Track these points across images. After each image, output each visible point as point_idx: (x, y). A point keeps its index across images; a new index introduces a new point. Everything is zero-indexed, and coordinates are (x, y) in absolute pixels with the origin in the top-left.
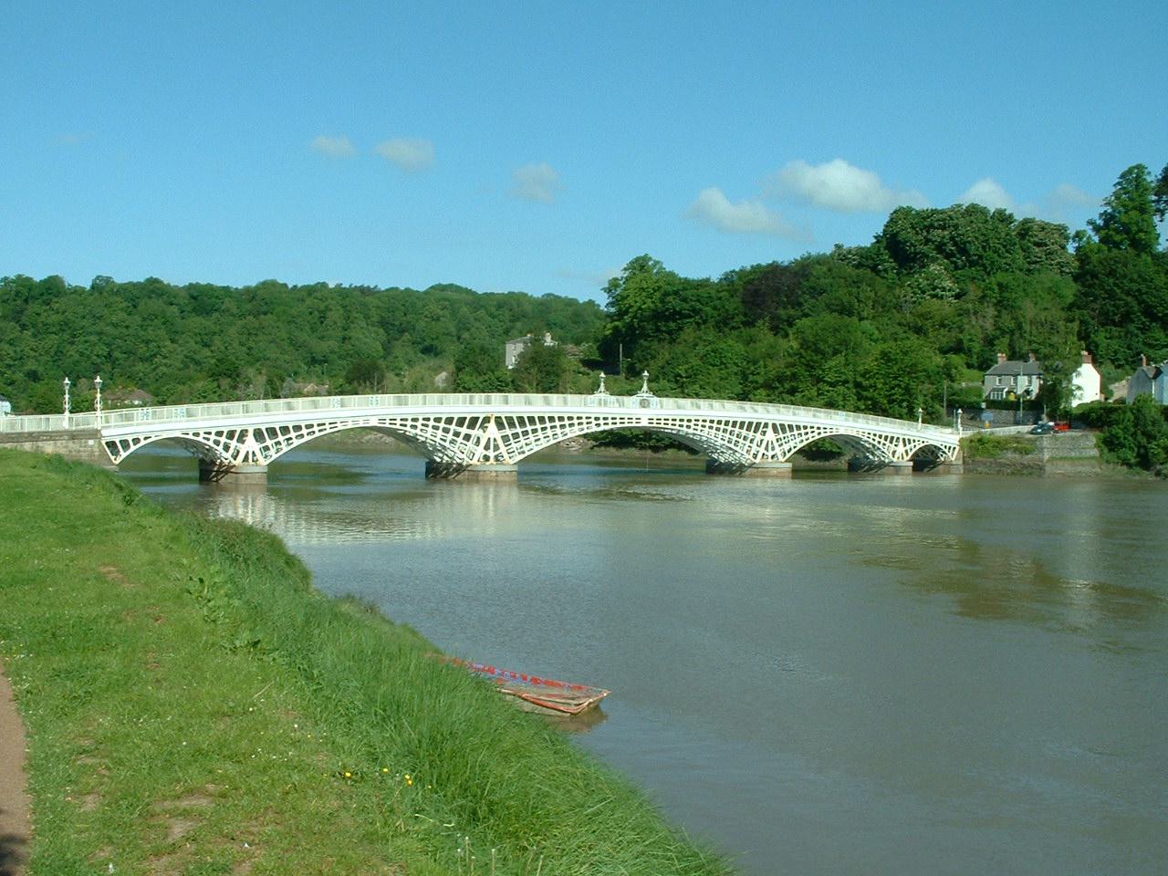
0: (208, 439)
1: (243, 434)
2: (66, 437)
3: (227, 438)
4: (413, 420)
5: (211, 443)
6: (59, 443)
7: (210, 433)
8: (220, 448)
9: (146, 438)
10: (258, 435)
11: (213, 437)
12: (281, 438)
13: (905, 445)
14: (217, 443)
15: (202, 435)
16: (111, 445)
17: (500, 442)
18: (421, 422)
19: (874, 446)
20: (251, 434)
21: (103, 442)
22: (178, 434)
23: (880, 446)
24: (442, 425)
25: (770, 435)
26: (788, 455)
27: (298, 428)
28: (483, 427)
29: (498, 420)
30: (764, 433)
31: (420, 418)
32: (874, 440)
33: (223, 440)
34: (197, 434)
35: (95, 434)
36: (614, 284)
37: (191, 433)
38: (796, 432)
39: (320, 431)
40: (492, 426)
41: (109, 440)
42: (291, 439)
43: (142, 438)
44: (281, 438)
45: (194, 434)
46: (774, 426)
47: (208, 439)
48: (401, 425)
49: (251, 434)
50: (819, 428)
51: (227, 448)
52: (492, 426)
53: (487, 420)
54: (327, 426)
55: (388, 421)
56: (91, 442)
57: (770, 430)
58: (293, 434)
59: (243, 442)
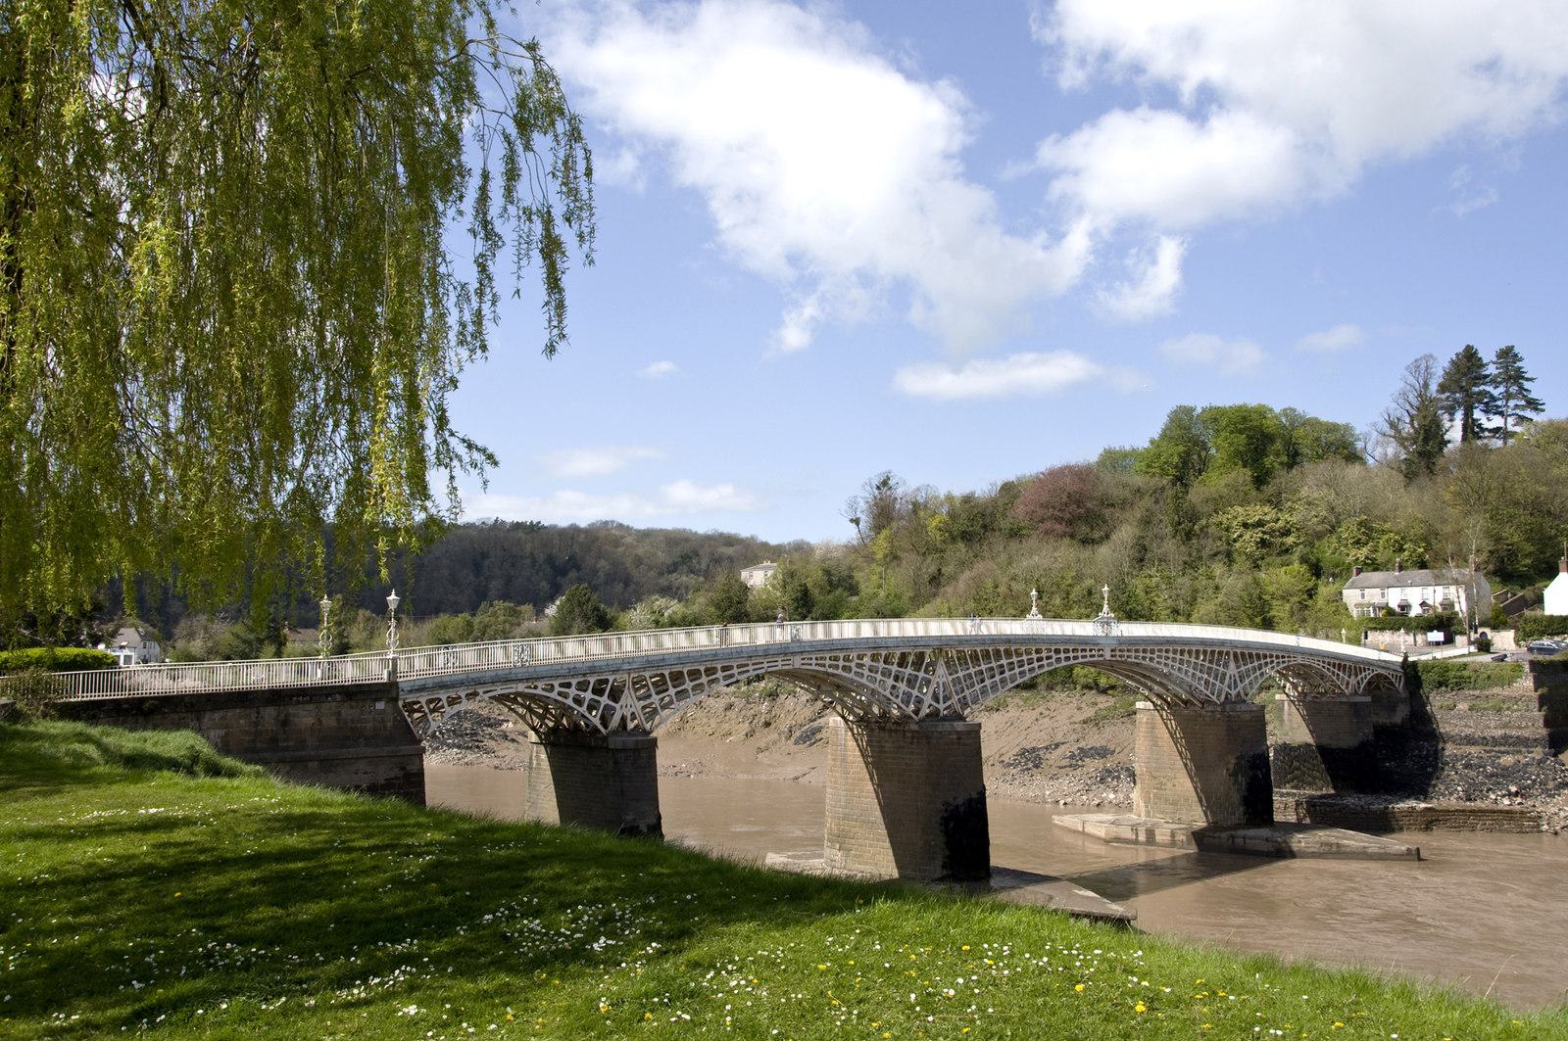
0: (566, 696)
3: (594, 692)
7: (568, 685)
8: (583, 709)
11: (573, 692)
12: (672, 691)
14: (578, 701)
15: (557, 689)
22: (521, 687)
25: (1232, 670)
30: (1226, 665)
33: (588, 695)
35: (388, 690)
38: (1256, 664)
41: (411, 698)
42: (685, 691)
46: (1235, 654)
47: (566, 696)
50: (1277, 657)
55: (814, 662)
56: (380, 705)
57: (1232, 665)
58: (688, 685)
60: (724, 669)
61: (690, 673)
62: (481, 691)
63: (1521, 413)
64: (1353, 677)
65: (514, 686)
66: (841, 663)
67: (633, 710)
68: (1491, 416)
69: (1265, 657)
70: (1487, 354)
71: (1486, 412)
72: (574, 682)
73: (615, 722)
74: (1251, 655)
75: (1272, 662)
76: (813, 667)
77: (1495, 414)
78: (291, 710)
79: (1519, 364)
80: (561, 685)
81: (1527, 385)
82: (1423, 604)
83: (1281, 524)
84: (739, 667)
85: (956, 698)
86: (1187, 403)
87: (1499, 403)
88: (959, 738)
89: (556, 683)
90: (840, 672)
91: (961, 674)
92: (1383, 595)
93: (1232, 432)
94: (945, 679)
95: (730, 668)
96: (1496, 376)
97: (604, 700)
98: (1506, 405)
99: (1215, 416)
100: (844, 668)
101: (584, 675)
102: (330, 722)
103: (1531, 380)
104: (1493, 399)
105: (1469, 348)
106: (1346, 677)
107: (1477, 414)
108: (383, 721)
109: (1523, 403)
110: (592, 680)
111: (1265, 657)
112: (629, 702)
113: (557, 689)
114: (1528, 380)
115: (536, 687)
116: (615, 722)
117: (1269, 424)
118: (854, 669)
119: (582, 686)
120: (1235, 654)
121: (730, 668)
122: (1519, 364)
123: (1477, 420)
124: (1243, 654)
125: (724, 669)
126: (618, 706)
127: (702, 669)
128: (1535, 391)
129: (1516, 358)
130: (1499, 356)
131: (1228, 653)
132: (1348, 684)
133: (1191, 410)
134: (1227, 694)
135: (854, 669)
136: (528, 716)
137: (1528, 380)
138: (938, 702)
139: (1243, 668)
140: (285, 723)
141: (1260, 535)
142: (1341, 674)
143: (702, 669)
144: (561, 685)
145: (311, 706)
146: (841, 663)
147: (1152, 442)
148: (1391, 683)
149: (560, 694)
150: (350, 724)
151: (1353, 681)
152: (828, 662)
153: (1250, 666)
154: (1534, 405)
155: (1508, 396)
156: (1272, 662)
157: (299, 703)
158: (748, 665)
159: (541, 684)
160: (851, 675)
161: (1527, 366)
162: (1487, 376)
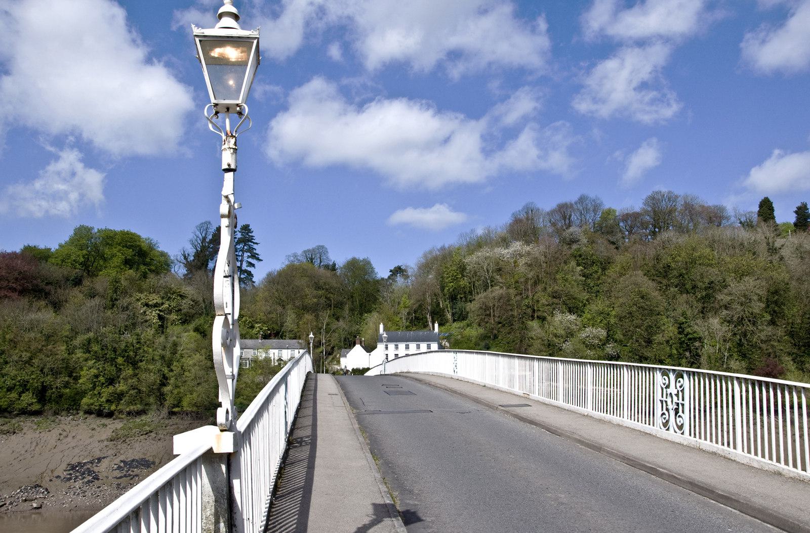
63: (250, 260)
79: (250, 234)
81: (255, 246)
83: (166, 306)
93: (123, 247)
98: (242, 256)
99: (110, 238)
103: (257, 243)
109: (250, 255)
114: (254, 243)
128: (258, 249)
129: (250, 231)
137: (254, 243)
141: (157, 312)
147: (61, 246)
161: (257, 235)
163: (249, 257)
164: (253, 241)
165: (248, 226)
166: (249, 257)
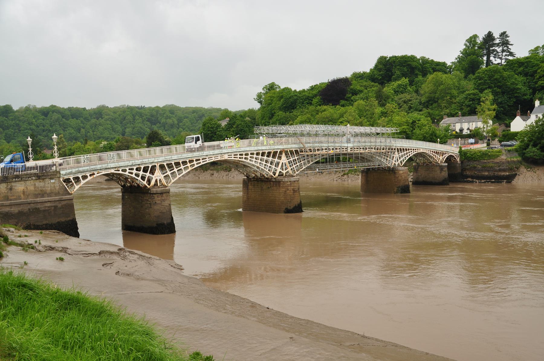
0: (132, 173)
1: (153, 168)
2: (34, 178)
3: (144, 171)
4: (251, 154)
5: (133, 176)
6: (28, 183)
7: (132, 169)
8: (139, 178)
9: (90, 175)
10: (162, 167)
11: (134, 172)
12: (176, 170)
13: (442, 156)
14: (137, 175)
15: (128, 171)
16: (67, 181)
17: (288, 165)
18: (250, 155)
19: (430, 156)
20: (158, 167)
21: (61, 179)
22: (113, 171)
23: (434, 157)
24: (255, 156)
26: (403, 163)
27: (184, 163)
28: (280, 158)
29: (286, 154)
31: (249, 153)
32: (432, 154)
33: (141, 173)
34: (125, 171)
36: (259, 96)
37: (121, 169)
38: (405, 152)
39: (197, 164)
40: (283, 156)
41: (66, 177)
43: (88, 175)
44: (176, 170)
45: (122, 170)
46: (398, 149)
47: (132, 173)
48: (240, 158)
49: (158, 167)
51: (143, 178)
52: (283, 156)
53: (281, 153)
54: (201, 161)
57: (396, 153)
58: (182, 167)
59: (153, 174)
60: (197, 160)
61: (183, 162)
62: (96, 173)
64: (441, 156)
65: (110, 170)
66: (244, 156)
67: (160, 178)
68: (496, 59)
69: (409, 150)
70: (496, 35)
71: (494, 57)
72: (135, 168)
73: (153, 183)
74: (403, 149)
75: (411, 152)
76: (233, 158)
77: (498, 58)
78: (13, 184)
79: (507, 39)
80: (129, 169)
81: (510, 47)
82: (468, 129)
84: (202, 159)
85: (290, 168)
86: (385, 55)
87: (500, 54)
88: (291, 184)
89: (127, 169)
90: (243, 160)
91: (292, 159)
92: (454, 126)
93: (401, 66)
94: (285, 162)
95: (199, 160)
96: (499, 43)
97: (148, 174)
98: (502, 55)
100: (245, 158)
101: (139, 165)
102: (32, 188)
103: (512, 45)
104: (498, 52)
105: (490, 33)
106: (438, 156)
107: (492, 58)
108: (54, 187)
109: (508, 54)
110: (142, 167)
111: (409, 150)
112: (158, 175)
113: (128, 171)
115: (119, 170)
116: (153, 183)
117: (414, 64)
118: (249, 159)
119: (138, 169)
120: (398, 149)
121: (199, 160)
122: (507, 39)
123: (492, 60)
124: (400, 149)
125: (197, 160)
126: (153, 176)
127: (188, 161)
128: (513, 49)
129: (507, 36)
130: (500, 36)
131: (395, 149)
132: (439, 159)
133: (386, 58)
134: (395, 164)
135: (249, 159)
136: (120, 182)
138: (283, 170)
139: (400, 154)
140: (11, 189)
142: (437, 155)
143: (188, 161)
144: (129, 169)
145: (22, 182)
146: (244, 156)
148: (455, 158)
149: (129, 173)
150: (40, 189)
151: (441, 158)
152: (238, 156)
153: (403, 153)
154: (511, 54)
155: (503, 51)
156: (411, 152)
157: (16, 181)
158: (206, 158)
159: (121, 169)
160: (248, 161)
161: (510, 39)
162: (496, 44)
163: (506, 55)
164: (510, 43)
165: (505, 33)
166: (506, 55)
